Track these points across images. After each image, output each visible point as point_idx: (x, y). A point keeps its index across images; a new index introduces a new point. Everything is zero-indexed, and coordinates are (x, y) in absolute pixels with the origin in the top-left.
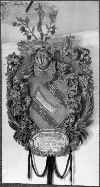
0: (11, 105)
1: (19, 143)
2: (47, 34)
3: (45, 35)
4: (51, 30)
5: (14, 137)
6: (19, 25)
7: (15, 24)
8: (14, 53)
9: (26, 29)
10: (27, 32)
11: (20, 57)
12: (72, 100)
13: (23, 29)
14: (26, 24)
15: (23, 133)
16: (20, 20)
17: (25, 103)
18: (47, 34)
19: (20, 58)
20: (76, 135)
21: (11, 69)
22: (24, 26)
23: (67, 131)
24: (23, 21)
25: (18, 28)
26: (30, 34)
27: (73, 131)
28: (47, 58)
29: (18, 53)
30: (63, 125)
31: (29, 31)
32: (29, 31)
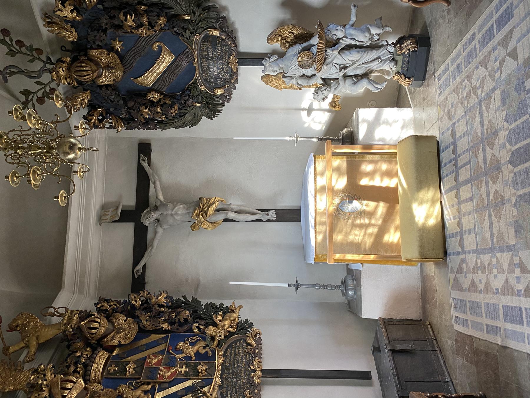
0: (163, 122)
1: (220, 111)
2: (44, 62)
3: (45, 66)
4: (34, 53)
5: (211, 119)
8: (85, 117)
9: (40, 94)
10: (45, 94)
11: (90, 109)
12: (145, 20)
14: (32, 95)
15: (205, 104)
17: (160, 100)
18: (44, 62)
19: (91, 107)
20: (202, 15)
21: (111, 123)
22: (35, 98)
23: (196, 32)
24: (27, 100)
26: (48, 89)
27: (195, 21)
28: (82, 62)
29: (85, 112)
30: (187, 38)
31: (43, 90)
32: (43, 90)
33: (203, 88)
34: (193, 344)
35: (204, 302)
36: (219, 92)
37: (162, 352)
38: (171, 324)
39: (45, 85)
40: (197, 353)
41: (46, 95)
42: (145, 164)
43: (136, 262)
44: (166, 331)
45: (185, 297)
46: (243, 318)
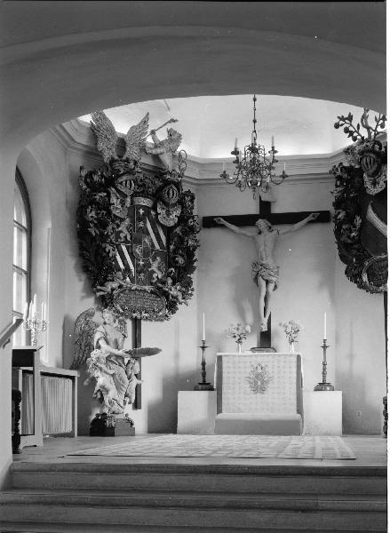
6: (342, 125)
7: (337, 126)
9: (351, 129)
13: (346, 130)
16: (342, 119)
17: (355, 227)
25: (342, 128)
26: (355, 134)
29: (346, 164)
33: (367, 264)
34: (159, 268)
35: (192, 276)
36: (365, 278)
37: (153, 245)
38: (174, 251)
39: (358, 132)
40: (153, 272)
41: (351, 134)
42: (310, 218)
43: (226, 218)
44: (169, 248)
45: (196, 260)
46: (179, 306)
